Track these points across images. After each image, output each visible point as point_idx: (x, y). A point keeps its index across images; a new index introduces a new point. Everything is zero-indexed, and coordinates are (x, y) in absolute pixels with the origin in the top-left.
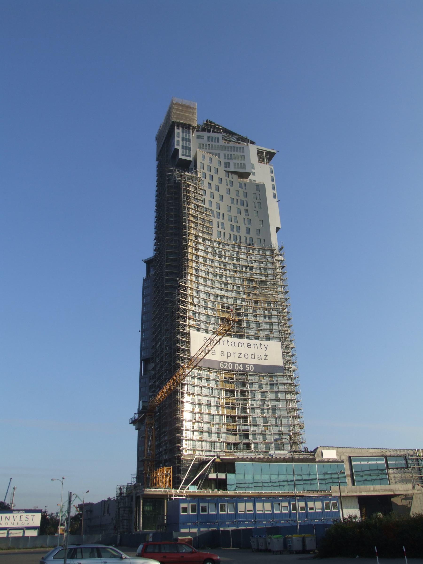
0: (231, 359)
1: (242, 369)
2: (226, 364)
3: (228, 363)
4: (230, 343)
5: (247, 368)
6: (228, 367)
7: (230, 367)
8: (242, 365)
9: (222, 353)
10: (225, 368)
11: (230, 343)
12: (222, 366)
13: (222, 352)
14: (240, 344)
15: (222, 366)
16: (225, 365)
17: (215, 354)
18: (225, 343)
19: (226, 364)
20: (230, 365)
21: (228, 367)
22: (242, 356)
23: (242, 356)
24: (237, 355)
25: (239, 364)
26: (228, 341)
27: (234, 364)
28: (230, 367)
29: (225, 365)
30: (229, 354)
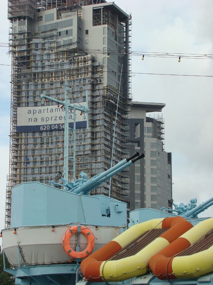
0: (49, 123)
1: (57, 128)
2: (45, 127)
3: (46, 125)
4: (49, 111)
5: (61, 127)
6: (46, 128)
7: (48, 128)
8: (57, 125)
9: (42, 119)
10: (44, 129)
11: (49, 111)
12: (42, 129)
13: (43, 119)
14: (57, 110)
15: (42, 129)
16: (44, 128)
17: (37, 121)
18: (46, 111)
19: (45, 127)
20: (48, 127)
21: (46, 128)
22: (58, 118)
23: (58, 118)
24: (53, 119)
25: (55, 125)
26: (47, 109)
27: (51, 125)
28: (48, 128)
29: (44, 128)
30: (48, 119)
